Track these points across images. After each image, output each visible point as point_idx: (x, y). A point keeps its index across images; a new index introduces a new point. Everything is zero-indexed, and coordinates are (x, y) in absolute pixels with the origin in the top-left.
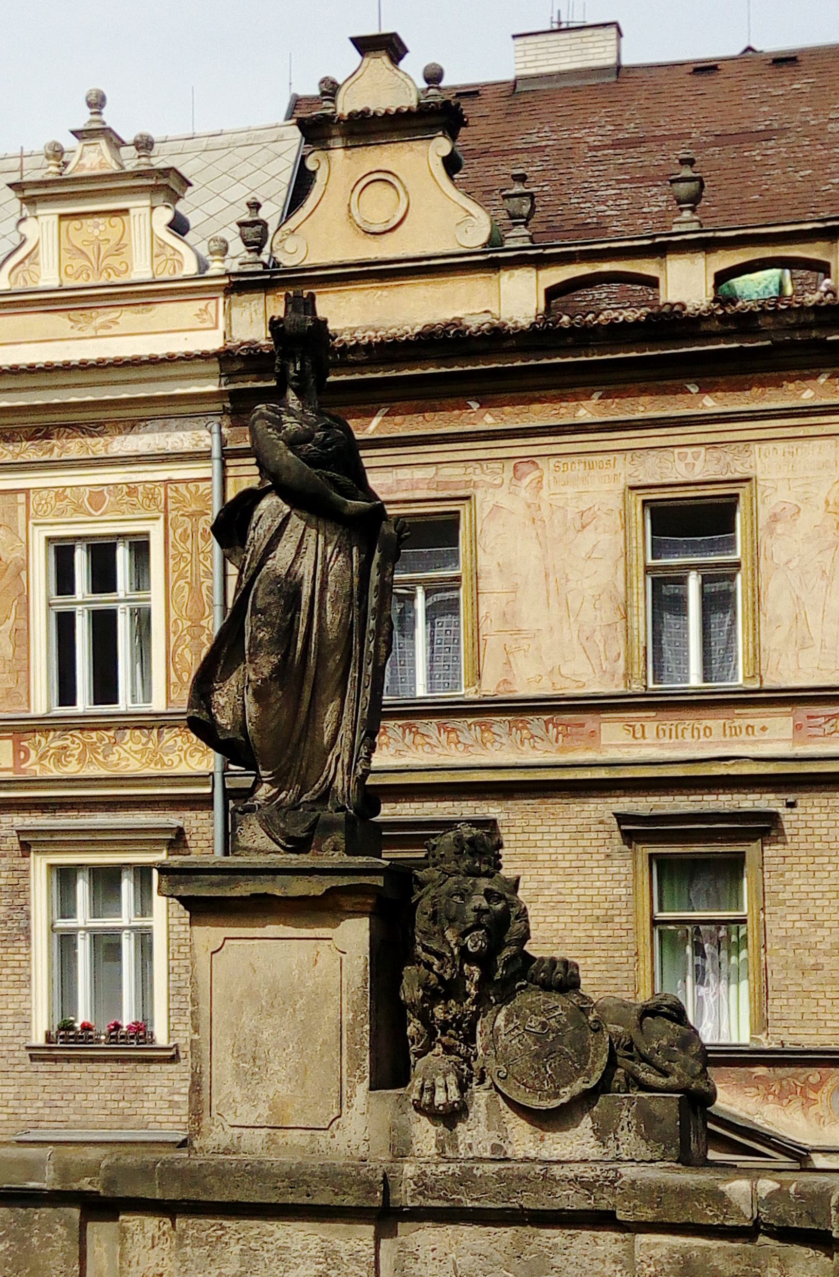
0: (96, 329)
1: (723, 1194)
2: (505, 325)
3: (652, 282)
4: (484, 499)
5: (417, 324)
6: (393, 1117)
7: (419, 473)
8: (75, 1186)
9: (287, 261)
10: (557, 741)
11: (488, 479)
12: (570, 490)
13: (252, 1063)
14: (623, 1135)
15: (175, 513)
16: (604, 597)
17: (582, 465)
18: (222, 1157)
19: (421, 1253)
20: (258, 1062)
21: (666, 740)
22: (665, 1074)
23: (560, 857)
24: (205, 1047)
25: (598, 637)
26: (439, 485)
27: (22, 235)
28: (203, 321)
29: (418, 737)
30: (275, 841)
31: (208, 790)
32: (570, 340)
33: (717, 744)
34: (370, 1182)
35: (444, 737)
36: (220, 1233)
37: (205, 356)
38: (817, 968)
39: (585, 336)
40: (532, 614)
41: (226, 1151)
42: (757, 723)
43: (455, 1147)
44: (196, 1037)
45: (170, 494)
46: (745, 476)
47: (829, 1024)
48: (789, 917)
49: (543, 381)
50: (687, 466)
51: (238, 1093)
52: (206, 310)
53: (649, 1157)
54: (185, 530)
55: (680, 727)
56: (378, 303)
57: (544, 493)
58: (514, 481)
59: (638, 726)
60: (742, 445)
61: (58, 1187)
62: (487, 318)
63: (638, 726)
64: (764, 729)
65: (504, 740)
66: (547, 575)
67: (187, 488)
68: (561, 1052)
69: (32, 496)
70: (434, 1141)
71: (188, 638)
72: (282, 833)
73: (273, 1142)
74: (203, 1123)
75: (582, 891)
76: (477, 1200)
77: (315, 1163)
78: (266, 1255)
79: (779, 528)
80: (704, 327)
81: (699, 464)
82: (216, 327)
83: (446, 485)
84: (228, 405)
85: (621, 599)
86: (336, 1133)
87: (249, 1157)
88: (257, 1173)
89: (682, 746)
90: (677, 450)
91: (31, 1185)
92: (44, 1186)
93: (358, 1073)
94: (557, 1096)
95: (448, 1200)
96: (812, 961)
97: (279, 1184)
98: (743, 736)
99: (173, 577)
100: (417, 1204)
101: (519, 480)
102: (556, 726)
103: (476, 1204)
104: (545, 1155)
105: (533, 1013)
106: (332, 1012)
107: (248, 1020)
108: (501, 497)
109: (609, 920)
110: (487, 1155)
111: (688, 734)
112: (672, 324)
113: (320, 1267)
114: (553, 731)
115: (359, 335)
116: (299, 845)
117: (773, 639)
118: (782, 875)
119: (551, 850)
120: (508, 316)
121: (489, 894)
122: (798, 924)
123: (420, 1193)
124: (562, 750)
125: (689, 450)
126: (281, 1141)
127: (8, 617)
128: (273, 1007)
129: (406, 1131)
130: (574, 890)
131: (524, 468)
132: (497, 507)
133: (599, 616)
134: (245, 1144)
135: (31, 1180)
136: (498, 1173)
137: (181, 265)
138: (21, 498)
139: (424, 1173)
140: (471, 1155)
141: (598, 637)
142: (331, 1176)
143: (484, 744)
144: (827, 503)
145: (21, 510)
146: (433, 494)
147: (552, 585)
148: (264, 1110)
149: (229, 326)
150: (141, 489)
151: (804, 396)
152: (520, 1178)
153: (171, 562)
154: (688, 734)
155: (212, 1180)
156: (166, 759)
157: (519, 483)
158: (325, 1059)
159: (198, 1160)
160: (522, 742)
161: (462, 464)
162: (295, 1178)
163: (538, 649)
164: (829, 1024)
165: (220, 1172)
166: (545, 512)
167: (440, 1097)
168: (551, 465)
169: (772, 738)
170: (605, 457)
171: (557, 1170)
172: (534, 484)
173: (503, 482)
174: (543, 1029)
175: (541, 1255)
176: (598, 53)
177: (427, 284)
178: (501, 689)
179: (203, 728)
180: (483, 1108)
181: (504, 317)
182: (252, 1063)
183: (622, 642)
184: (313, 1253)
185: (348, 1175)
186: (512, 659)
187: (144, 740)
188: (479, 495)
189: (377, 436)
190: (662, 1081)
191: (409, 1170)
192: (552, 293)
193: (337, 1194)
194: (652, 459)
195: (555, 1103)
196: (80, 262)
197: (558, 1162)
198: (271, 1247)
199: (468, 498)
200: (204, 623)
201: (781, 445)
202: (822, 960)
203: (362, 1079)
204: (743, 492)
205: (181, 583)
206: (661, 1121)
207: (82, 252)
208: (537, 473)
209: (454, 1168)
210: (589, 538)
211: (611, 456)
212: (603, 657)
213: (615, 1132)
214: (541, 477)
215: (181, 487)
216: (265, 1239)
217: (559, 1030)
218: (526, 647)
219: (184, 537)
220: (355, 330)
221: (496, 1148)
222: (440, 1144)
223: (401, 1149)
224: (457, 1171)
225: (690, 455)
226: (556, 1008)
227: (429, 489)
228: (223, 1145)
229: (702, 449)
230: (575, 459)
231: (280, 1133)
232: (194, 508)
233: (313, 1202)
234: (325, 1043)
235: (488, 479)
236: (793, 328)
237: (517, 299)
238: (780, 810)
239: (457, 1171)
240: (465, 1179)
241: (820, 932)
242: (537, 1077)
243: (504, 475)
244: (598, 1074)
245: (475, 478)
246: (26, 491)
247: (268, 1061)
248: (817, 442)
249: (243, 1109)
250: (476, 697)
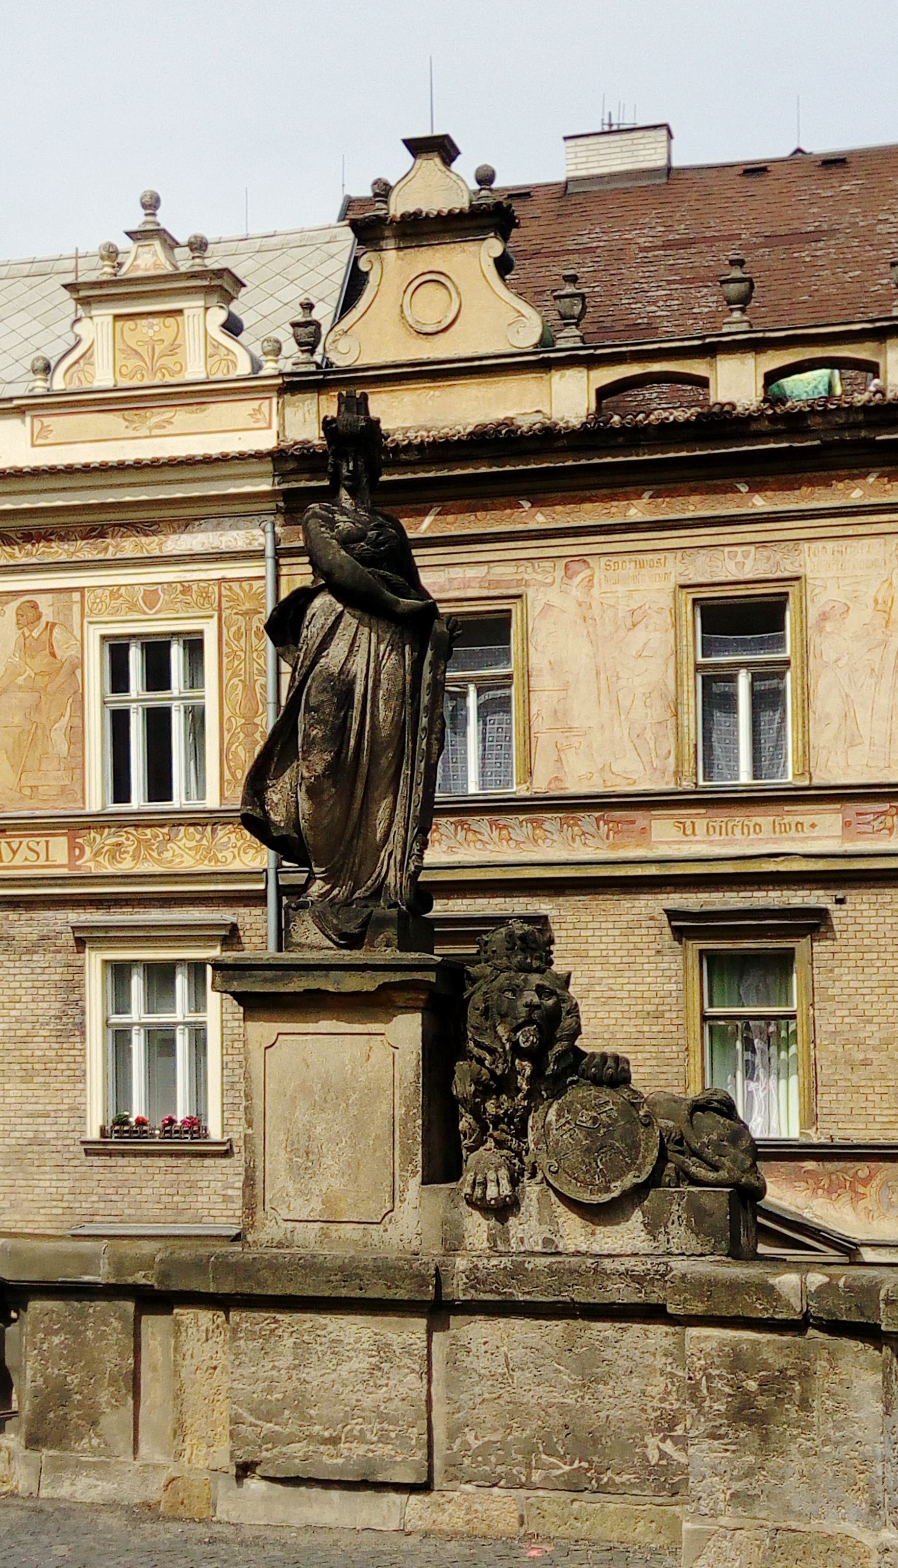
0: (150, 429)
1: (772, 1287)
2: (556, 424)
3: (702, 382)
4: (536, 598)
5: (469, 424)
6: (445, 1211)
7: (471, 572)
8: (130, 1280)
9: (340, 361)
10: (608, 838)
11: (539, 577)
12: (621, 589)
13: (305, 1158)
14: (673, 1229)
15: (229, 611)
16: (655, 695)
17: (633, 564)
18: (275, 1250)
19: (473, 1346)
20: (311, 1157)
21: (716, 837)
22: (715, 1168)
23: (611, 953)
24: (259, 1142)
25: (648, 734)
26: (491, 584)
27: (77, 336)
28: (257, 421)
29: (470, 834)
30: (328, 937)
31: (261, 886)
32: (620, 440)
33: (767, 841)
34: (423, 1276)
35: (496, 833)
36: (273, 1326)
37: (259, 456)
38: (866, 1063)
39: (636, 436)
40: (584, 710)
41: (280, 1245)
42: (807, 820)
43: (507, 1241)
44: (250, 1131)
45: (224, 592)
46: (795, 575)
47: (878, 1119)
48: (838, 1013)
49: (594, 480)
50: (736, 564)
51: (291, 1188)
52: (259, 410)
53: (699, 1250)
54: (239, 628)
55: (730, 824)
56: (430, 403)
57: (595, 592)
58: (566, 580)
59: (688, 822)
60: (791, 544)
61: (113, 1281)
62: (538, 418)
63: (688, 822)
64: (813, 826)
65: (555, 837)
66: (598, 673)
67: (241, 586)
68: (612, 1146)
69: (87, 594)
70: (485, 1235)
71: (242, 735)
72: (335, 929)
73: (326, 1235)
74: (257, 1217)
75: (632, 987)
76: (529, 1293)
77: (368, 1257)
78: (319, 1348)
79: (829, 626)
80: (754, 427)
81: (749, 563)
82: (269, 427)
83: (498, 583)
84: (281, 504)
85: (672, 697)
86: (389, 1227)
87: (302, 1251)
88: (310, 1266)
89: (731, 843)
90: (727, 549)
91: (86, 1278)
92: (99, 1280)
93: (410, 1167)
94: (608, 1190)
95: (500, 1294)
96: (861, 1057)
97: (332, 1278)
98: (793, 833)
99: (226, 675)
100: (469, 1298)
101: (570, 578)
102: (607, 823)
103: (528, 1298)
104: (596, 1249)
105: (584, 1108)
106: (385, 1107)
107: (302, 1115)
108: (553, 596)
109: (659, 1016)
110: (539, 1248)
111: (738, 831)
112: (722, 423)
113: (373, 1360)
114: (604, 828)
115: (411, 434)
116: (352, 941)
117: (821, 737)
118: (831, 971)
119: (602, 946)
120: (560, 416)
121: (540, 990)
122: (847, 1020)
123: (472, 1287)
124: (613, 847)
125: (739, 549)
126: (334, 1235)
127: (63, 715)
128: (325, 1101)
129: (458, 1225)
130: (625, 986)
131: (575, 566)
132: (548, 606)
133: (649, 714)
134: (298, 1238)
135: (88, 1274)
136: (549, 1267)
137: (235, 365)
138: (76, 596)
139: (476, 1267)
140: (522, 1249)
141: (648, 734)
142: (384, 1270)
143: (536, 841)
144: (876, 601)
145: (76, 608)
146: (485, 593)
147: (603, 683)
148: (317, 1204)
149: (283, 426)
150: (195, 587)
151: (853, 495)
152: (572, 1272)
153: (225, 660)
154: (738, 831)
155: (265, 1274)
156: (219, 855)
157: (570, 582)
158: (378, 1154)
159: (252, 1253)
160: (573, 839)
161: (514, 563)
162: (348, 1272)
163: (589, 746)
164: (878, 1119)
165: (273, 1266)
166: (596, 610)
167: (492, 1192)
168: (602, 564)
169: (822, 835)
171: (608, 1264)
172: (585, 583)
174: (594, 1123)
175: (592, 1348)
176: (648, 155)
177: (479, 384)
178: (552, 786)
179: (257, 825)
180: (534, 1202)
181: (556, 417)
182: (305, 1158)
183: (672, 740)
184: (366, 1346)
185: (401, 1269)
186: (563, 757)
187: (198, 837)
188: (531, 593)
189: (429, 535)
190: (712, 1175)
191: (461, 1263)
192: (603, 393)
193: (389, 1288)
194: (702, 557)
195: (606, 1197)
196: (134, 362)
197: (609, 1256)
198: (324, 1340)
199: (519, 597)
200: (257, 720)
201: (830, 544)
202: (871, 1055)
203: (414, 1173)
204: (793, 590)
205: (235, 681)
206: (711, 1215)
207: (137, 352)
208: (588, 572)
209: (505, 1261)
210: (640, 636)
211: (662, 555)
212: (653, 755)
213: (666, 1226)
214: (592, 575)
215: (235, 586)
216: (318, 1332)
217: (610, 1125)
218: (577, 745)
219: (238, 636)
220: (407, 429)
221: (547, 1242)
222: (492, 1238)
223: (453, 1243)
224: (509, 1265)
225: (740, 554)
226: (607, 1103)
227: (481, 587)
228: (277, 1239)
229: (752, 548)
230: (626, 557)
231: (333, 1227)
232: (247, 606)
233: (366, 1296)
234: (377, 1137)
235: (539, 577)
236: (842, 428)
237: (569, 398)
238: (829, 907)
239: (509, 1265)
240: (516, 1273)
241: (869, 1028)
242: (588, 1172)
243: (556, 574)
244: (649, 1169)
245: (526, 577)
246: (81, 590)
247: (321, 1156)
248: (866, 541)
249: (297, 1203)
250: (527, 794)
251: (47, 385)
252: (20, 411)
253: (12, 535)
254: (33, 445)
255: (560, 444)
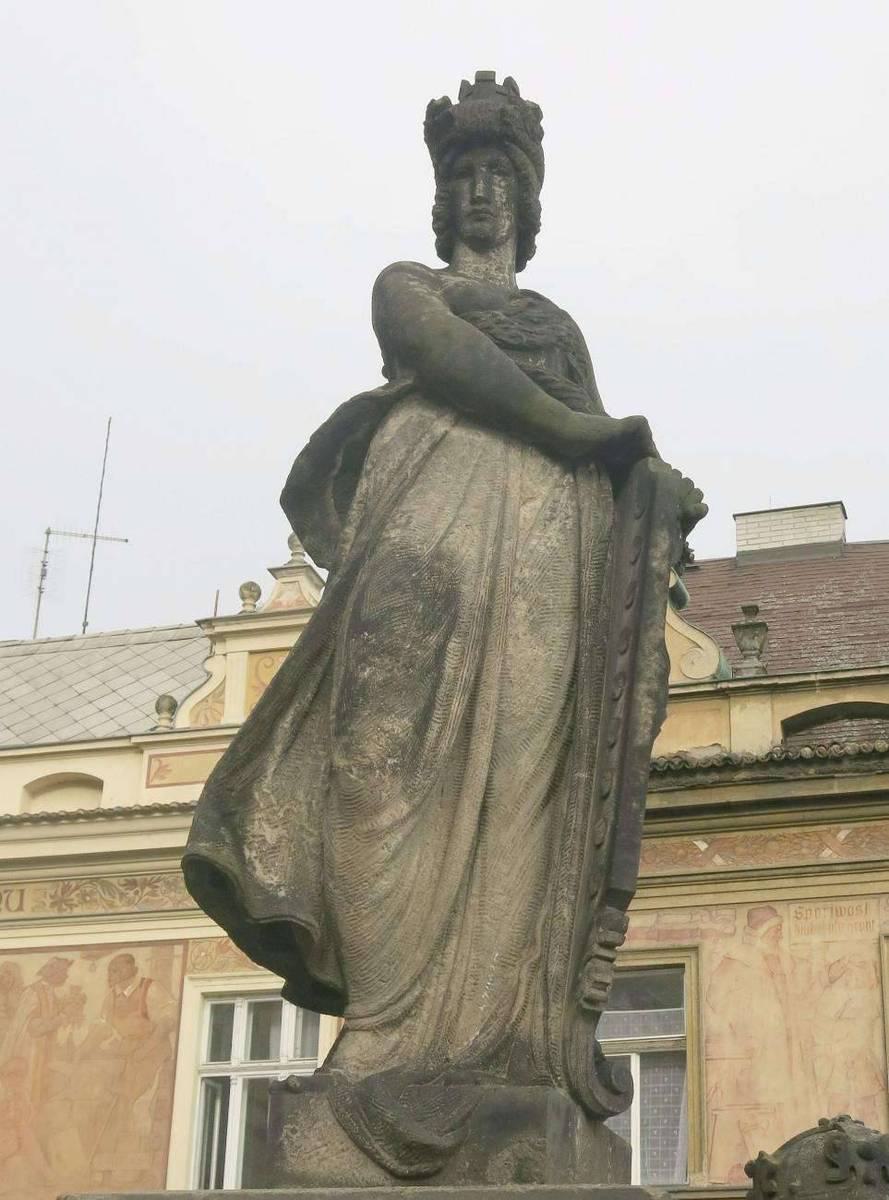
4: (714, 951)
11: (718, 927)
12: (816, 940)
17: (828, 913)
27: (208, 673)
30: (372, 1156)
32: (812, 771)
39: (828, 763)
57: (784, 944)
58: (748, 929)
62: (715, 751)
72: (393, 1137)
83: (669, 934)
108: (733, 948)
132: (728, 959)
146: (653, 944)
147: (796, 1049)
161: (688, 910)
166: (786, 965)
168: (792, 914)
170: (854, 903)
173: (735, 930)
176: (818, 532)
179: (214, 886)
181: (734, 751)
188: (707, 947)
199: (695, 949)
208: (773, 922)
210: (839, 995)
211: (863, 902)
230: (821, 904)
235: (718, 927)
243: (737, 923)
245: (703, 926)
250: (705, 1185)
251: (171, 725)
252: (138, 749)
253: (114, 881)
254: (148, 786)
255: (742, 775)
